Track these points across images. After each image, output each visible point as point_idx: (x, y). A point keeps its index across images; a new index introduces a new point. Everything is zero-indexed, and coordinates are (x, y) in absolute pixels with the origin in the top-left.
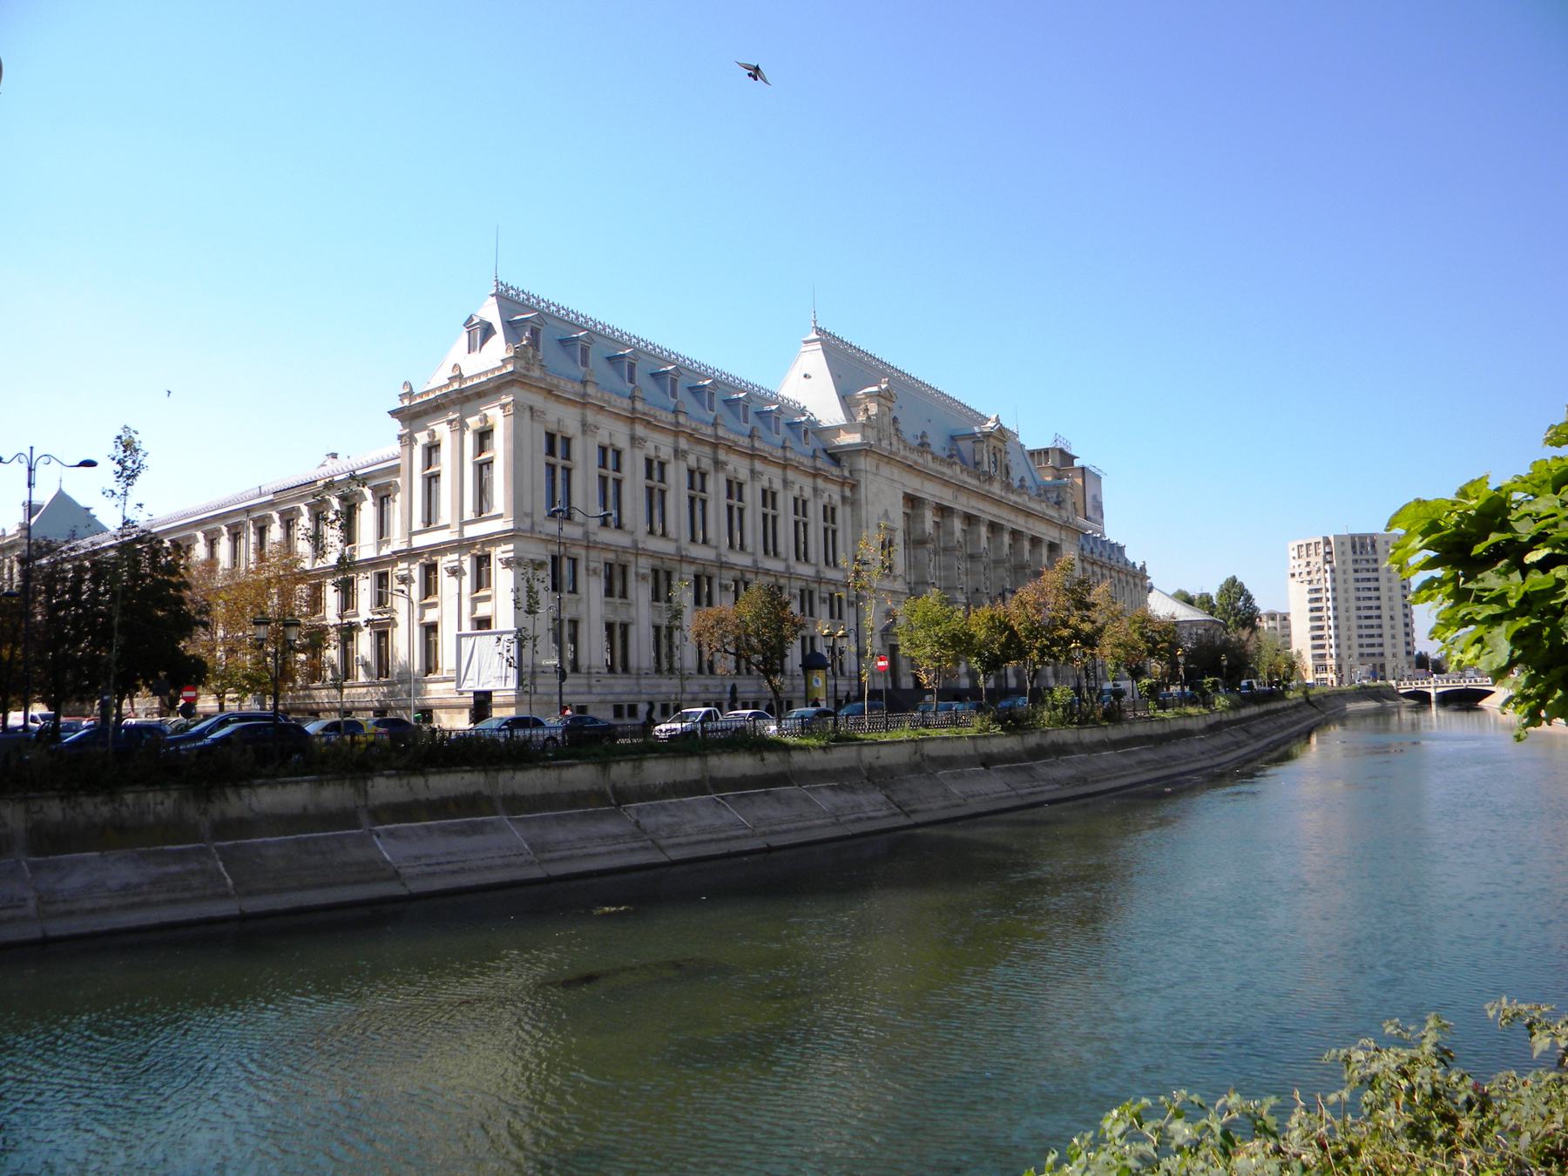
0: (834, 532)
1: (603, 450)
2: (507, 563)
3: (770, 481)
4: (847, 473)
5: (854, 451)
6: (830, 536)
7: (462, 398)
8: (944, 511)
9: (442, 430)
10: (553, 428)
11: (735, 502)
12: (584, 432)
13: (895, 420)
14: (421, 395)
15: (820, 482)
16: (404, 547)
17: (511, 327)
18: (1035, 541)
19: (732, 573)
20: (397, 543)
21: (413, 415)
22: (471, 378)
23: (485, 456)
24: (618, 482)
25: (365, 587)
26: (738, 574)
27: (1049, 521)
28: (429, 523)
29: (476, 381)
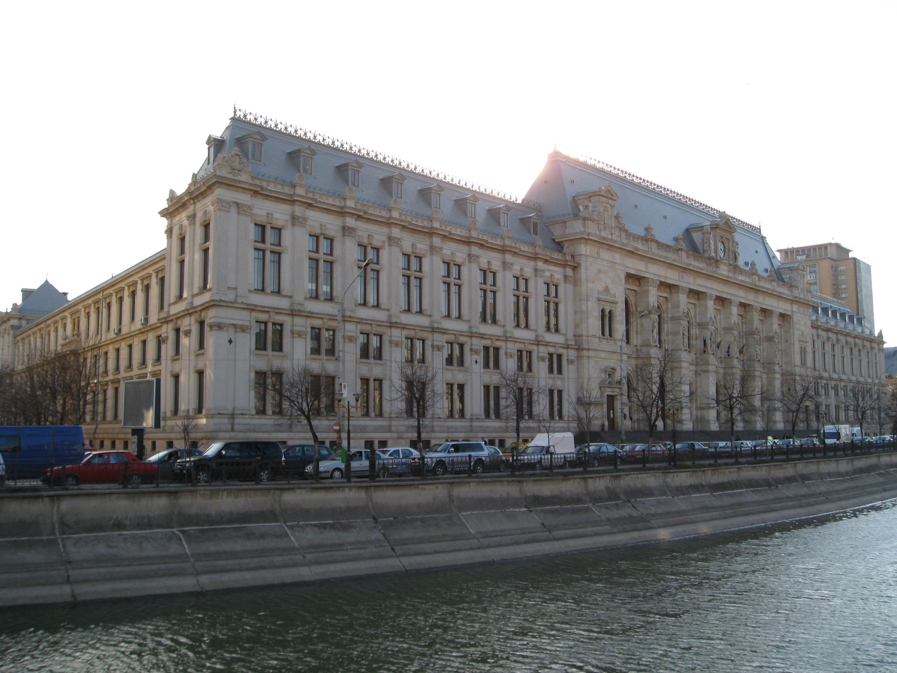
4: (568, 258)
6: (552, 308)
19: (446, 337)
27: (780, 297)
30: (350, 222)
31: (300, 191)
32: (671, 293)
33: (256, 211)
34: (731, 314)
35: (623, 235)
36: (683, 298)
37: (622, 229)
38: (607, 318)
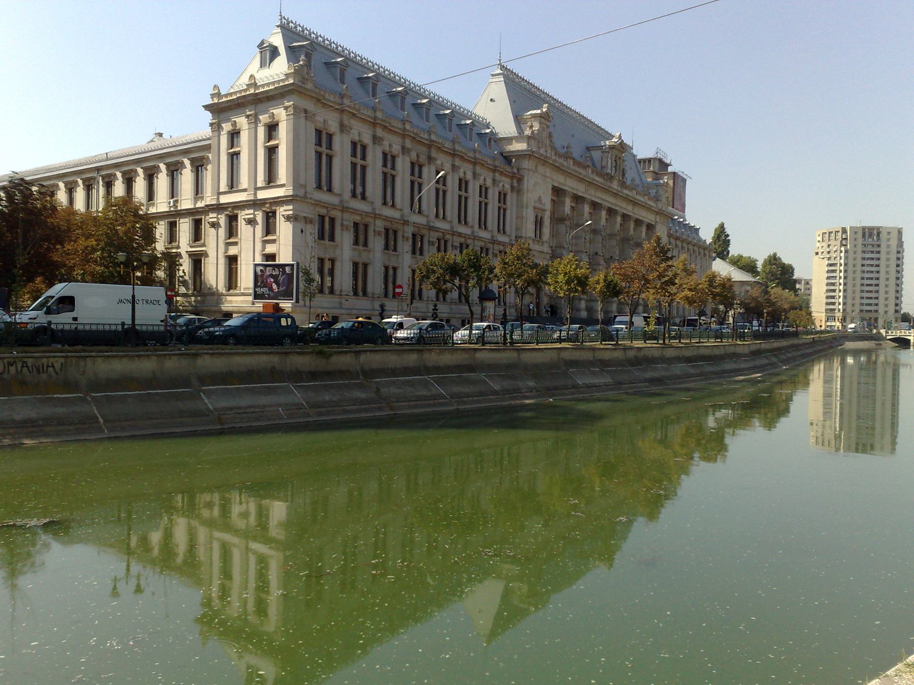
0: (505, 210)
1: (354, 144)
2: (288, 218)
3: (465, 173)
4: (515, 171)
5: (520, 155)
6: (502, 212)
7: (255, 101)
8: (578, 199)
9: (242, 121)
10: (320, 126)
12: (342, 131)
14: (226, 95)
16: (214, 202)
17: (292, 52)
18: (638, 222)
19: (437, 234)
20: (209, 199)
21: (221, 109)
22: (263, 86)
23: (272, 143)
24: (364, 168)
25: (185, 227)
26: (441, 234)
27: (649, 209)
28: (232, 187)
29: (266, 89)
30: (380, 132)
31: (347, 102)
33: (317, 118)
35: (553, 153)
37: (553, 148)
38: (539, 223)
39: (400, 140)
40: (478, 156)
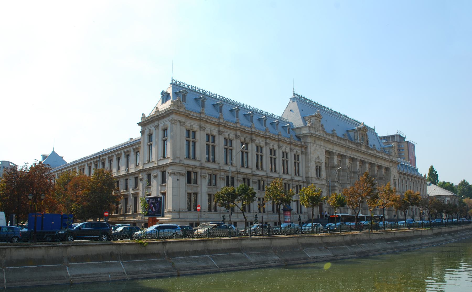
0: (298, 164)
4: (303, 144)
5: (306, 136)
6: (297, 164)
8: (342, 156)
10: (188, 128)
11: (259, 153)
13: (322, 125)
15: (292, 146)
16: (142, 168)
18: (380, 167)
19: (258, 178)
20: (140, 168)
25: (131, 182)
26: (260, 178)
27: (385, 160)
30: (222, 129)
32: (342, 158)
33: (186, 124)
34: (366, 167)
35: (324, 134)
36: (347, 161)
37: (324, 131)
38: (318, 169)
39: (234, 132)
40: (280, 137)
